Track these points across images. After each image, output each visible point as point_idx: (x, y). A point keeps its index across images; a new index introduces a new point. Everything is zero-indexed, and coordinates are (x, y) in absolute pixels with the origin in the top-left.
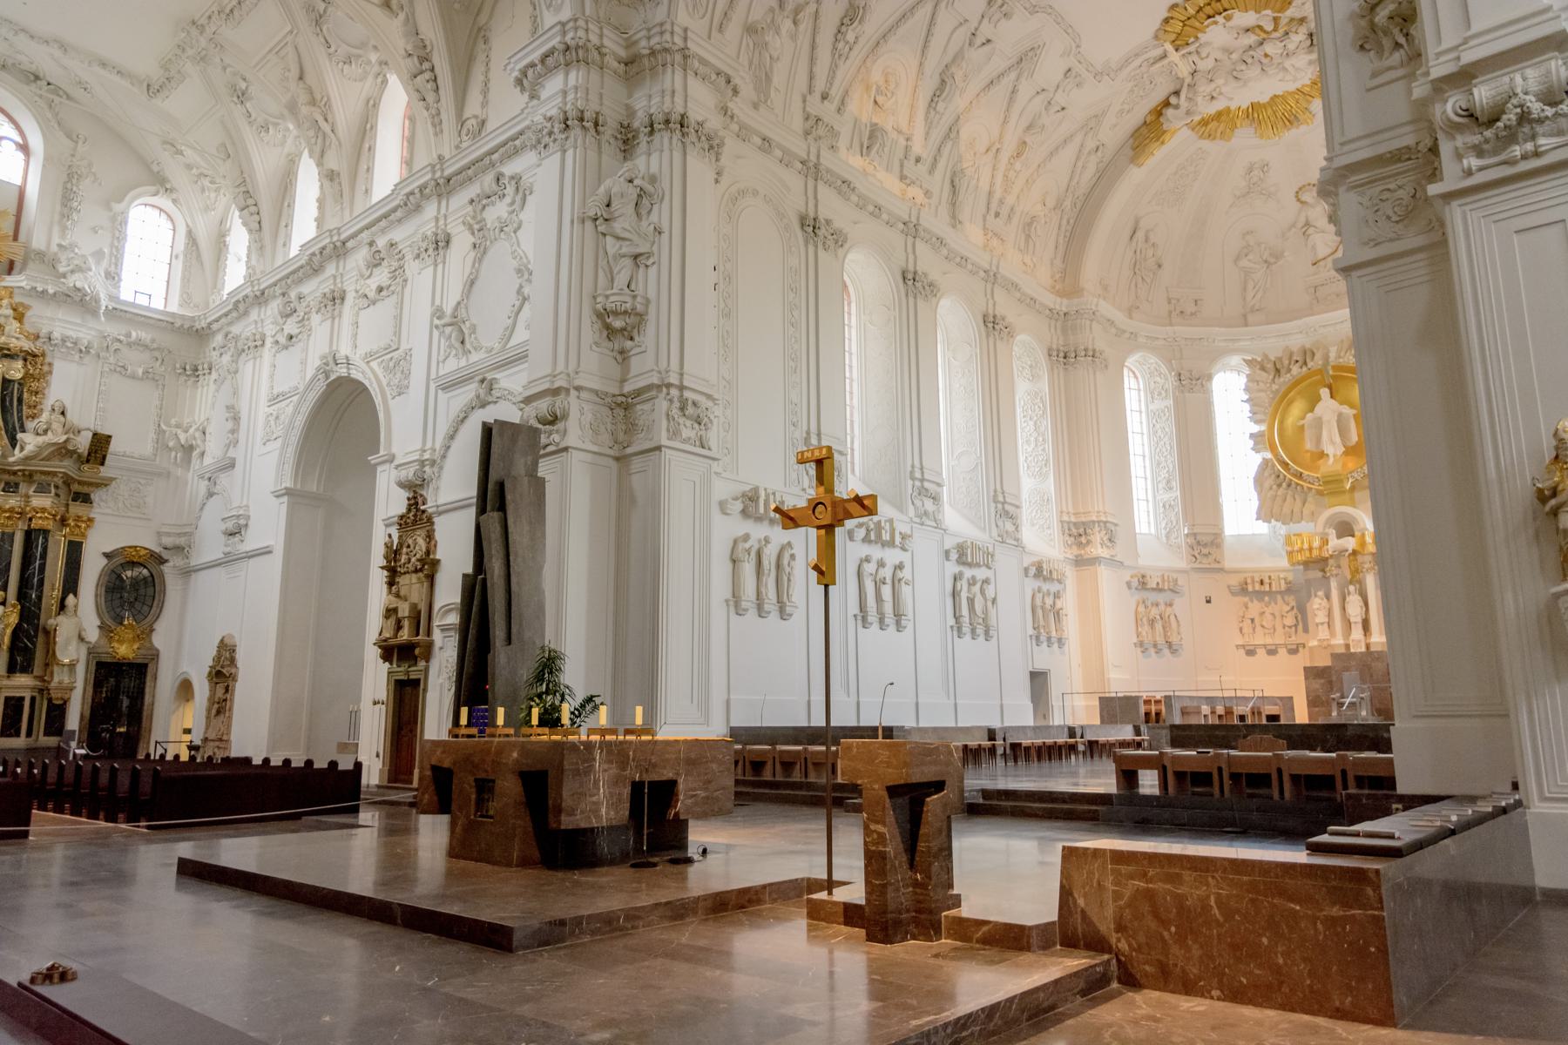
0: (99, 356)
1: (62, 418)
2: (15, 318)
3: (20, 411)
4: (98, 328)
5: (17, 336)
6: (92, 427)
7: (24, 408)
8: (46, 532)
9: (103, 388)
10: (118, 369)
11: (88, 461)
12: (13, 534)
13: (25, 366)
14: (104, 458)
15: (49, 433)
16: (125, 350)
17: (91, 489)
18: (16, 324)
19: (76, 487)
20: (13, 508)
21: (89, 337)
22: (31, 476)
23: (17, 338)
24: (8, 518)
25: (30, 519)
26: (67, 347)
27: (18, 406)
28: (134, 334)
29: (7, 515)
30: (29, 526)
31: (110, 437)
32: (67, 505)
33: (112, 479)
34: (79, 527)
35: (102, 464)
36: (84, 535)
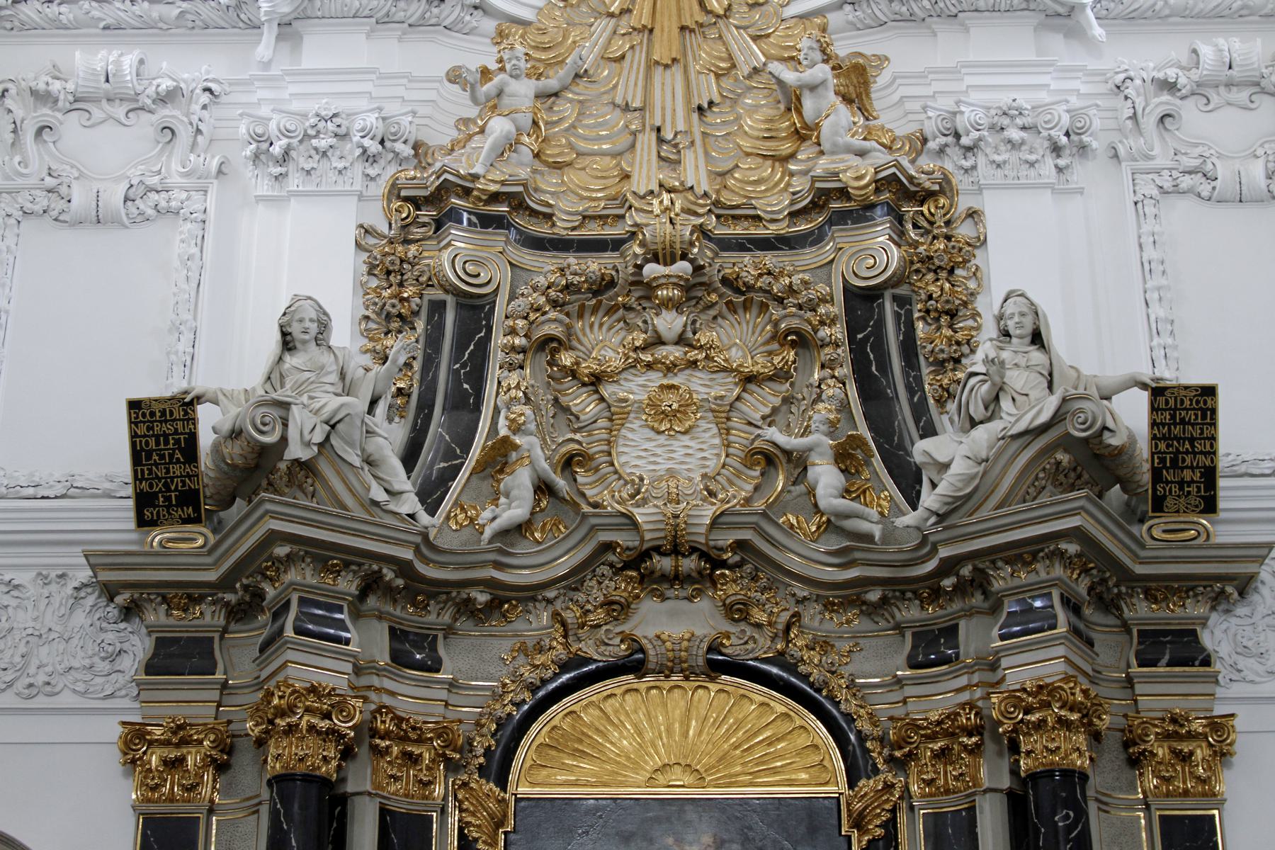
0: (1116, 156)
1: (1036, 356)
2: (847, 100)
3: (914, 387)
4: (1093, 65)
5: (857, 142)
6: (1146, 373)
7: (926, 370)
8: (1074, 779)
9: (1150, 253)
10: (1186, 182)
11: (1158, 505)
12: (971, 810)
13: (899, 237)
14: (1210, 475)
15: (1006, 404)
16: (1190, 112)
17: (1194, 609)
18: (844, 114)
19: (1140, 610)
20: (953, 716)
21: (1075, 102)
22: (980, 582)
23: (861, 154)
24: (942, 755)
25: (1014, 748)
26: (1013, 145)
27: (906, 375)
28: (1206, 52)
29: (937, 746)
30: (1014, 771)
31: (1210, 391)
32: (1129, 682)
33: (1258, 552)
34: (1186, 758)
35: (1210, 506)
36: (1212, 797)
